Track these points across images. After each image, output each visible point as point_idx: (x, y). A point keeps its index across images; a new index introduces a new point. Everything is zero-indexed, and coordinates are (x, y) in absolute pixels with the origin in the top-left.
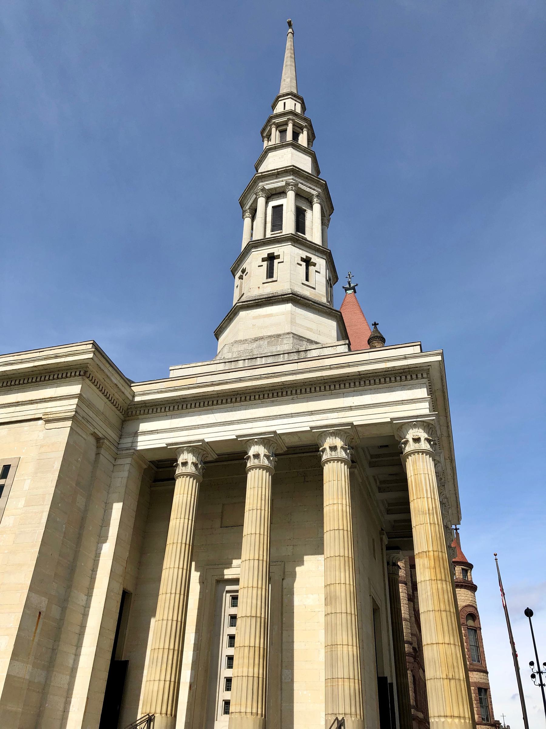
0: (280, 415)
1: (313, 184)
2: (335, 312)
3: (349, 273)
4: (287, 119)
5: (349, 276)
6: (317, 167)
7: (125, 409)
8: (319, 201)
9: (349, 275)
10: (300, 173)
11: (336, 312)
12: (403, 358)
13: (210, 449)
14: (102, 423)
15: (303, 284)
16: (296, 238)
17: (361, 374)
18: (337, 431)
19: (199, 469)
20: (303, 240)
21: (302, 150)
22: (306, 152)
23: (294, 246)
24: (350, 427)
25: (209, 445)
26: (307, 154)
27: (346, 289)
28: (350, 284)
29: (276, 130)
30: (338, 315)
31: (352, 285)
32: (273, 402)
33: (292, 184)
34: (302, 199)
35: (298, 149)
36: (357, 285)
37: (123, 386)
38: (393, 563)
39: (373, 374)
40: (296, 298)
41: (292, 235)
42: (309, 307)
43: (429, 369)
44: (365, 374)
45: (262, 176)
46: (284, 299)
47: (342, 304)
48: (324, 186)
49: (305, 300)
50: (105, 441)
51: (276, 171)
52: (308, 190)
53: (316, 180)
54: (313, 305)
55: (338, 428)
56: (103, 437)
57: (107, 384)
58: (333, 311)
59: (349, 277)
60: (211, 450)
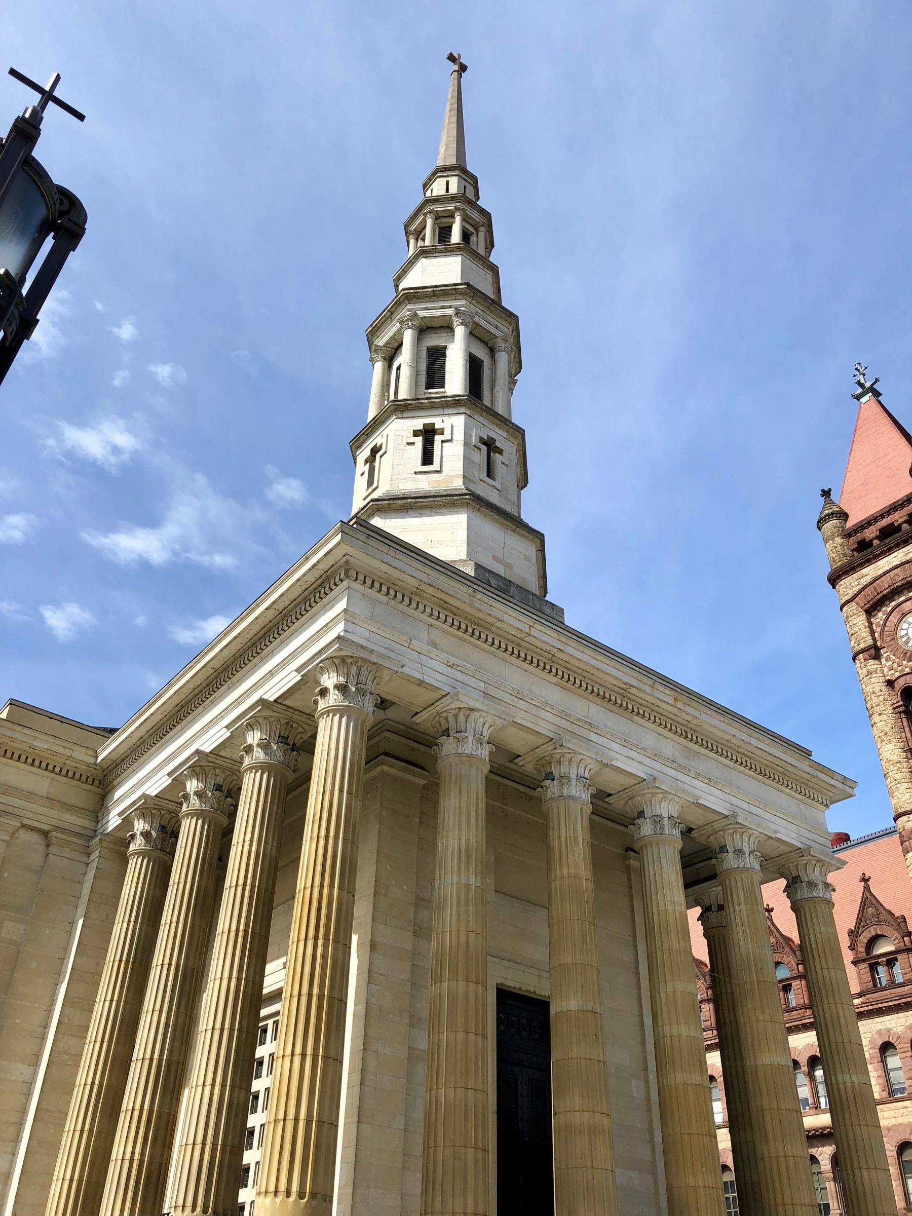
0: (211, 721)
1: (450, 299)
2: (458, 497)
3: (857, 366)
4: (453, 208)
5: (859, 371)
6: (484, 262)
8: (460, 321)
9: (856, 369)
10: (419, 294)
11: (461, 497)
13: (172, 804)
14: (46, 809)
16: (402, 405)
18: (252, 719)
20: (414, 402)
21: (442, 252)
22: (451, 251)
24: (260, 707)
25: (165, 799)
26: (452, 253)
27: (858, 397)
28: (861, 385)
29: (417, 240)
30: (468, 501)
31: (868, 385)
32: (212, 702)
33: (406, 318)
34: (439, 332)
36: (877, 380)
37: (65, 748)
39: (294, 603)
40: (381, 504)
41: (392, 403)
42: (411, 509)
43: (347, 561)
44: (285, 608)
45: (374, 330)
46: (368, 513)
47: (856, 427)
49: (397, 501)
50: (54, 834)
51: (386, 311)
52: (440, 312)
53: (449, 290)
54: (416, 503)
55: (251, 715)
58: (456, 498)
59: (858, 373)
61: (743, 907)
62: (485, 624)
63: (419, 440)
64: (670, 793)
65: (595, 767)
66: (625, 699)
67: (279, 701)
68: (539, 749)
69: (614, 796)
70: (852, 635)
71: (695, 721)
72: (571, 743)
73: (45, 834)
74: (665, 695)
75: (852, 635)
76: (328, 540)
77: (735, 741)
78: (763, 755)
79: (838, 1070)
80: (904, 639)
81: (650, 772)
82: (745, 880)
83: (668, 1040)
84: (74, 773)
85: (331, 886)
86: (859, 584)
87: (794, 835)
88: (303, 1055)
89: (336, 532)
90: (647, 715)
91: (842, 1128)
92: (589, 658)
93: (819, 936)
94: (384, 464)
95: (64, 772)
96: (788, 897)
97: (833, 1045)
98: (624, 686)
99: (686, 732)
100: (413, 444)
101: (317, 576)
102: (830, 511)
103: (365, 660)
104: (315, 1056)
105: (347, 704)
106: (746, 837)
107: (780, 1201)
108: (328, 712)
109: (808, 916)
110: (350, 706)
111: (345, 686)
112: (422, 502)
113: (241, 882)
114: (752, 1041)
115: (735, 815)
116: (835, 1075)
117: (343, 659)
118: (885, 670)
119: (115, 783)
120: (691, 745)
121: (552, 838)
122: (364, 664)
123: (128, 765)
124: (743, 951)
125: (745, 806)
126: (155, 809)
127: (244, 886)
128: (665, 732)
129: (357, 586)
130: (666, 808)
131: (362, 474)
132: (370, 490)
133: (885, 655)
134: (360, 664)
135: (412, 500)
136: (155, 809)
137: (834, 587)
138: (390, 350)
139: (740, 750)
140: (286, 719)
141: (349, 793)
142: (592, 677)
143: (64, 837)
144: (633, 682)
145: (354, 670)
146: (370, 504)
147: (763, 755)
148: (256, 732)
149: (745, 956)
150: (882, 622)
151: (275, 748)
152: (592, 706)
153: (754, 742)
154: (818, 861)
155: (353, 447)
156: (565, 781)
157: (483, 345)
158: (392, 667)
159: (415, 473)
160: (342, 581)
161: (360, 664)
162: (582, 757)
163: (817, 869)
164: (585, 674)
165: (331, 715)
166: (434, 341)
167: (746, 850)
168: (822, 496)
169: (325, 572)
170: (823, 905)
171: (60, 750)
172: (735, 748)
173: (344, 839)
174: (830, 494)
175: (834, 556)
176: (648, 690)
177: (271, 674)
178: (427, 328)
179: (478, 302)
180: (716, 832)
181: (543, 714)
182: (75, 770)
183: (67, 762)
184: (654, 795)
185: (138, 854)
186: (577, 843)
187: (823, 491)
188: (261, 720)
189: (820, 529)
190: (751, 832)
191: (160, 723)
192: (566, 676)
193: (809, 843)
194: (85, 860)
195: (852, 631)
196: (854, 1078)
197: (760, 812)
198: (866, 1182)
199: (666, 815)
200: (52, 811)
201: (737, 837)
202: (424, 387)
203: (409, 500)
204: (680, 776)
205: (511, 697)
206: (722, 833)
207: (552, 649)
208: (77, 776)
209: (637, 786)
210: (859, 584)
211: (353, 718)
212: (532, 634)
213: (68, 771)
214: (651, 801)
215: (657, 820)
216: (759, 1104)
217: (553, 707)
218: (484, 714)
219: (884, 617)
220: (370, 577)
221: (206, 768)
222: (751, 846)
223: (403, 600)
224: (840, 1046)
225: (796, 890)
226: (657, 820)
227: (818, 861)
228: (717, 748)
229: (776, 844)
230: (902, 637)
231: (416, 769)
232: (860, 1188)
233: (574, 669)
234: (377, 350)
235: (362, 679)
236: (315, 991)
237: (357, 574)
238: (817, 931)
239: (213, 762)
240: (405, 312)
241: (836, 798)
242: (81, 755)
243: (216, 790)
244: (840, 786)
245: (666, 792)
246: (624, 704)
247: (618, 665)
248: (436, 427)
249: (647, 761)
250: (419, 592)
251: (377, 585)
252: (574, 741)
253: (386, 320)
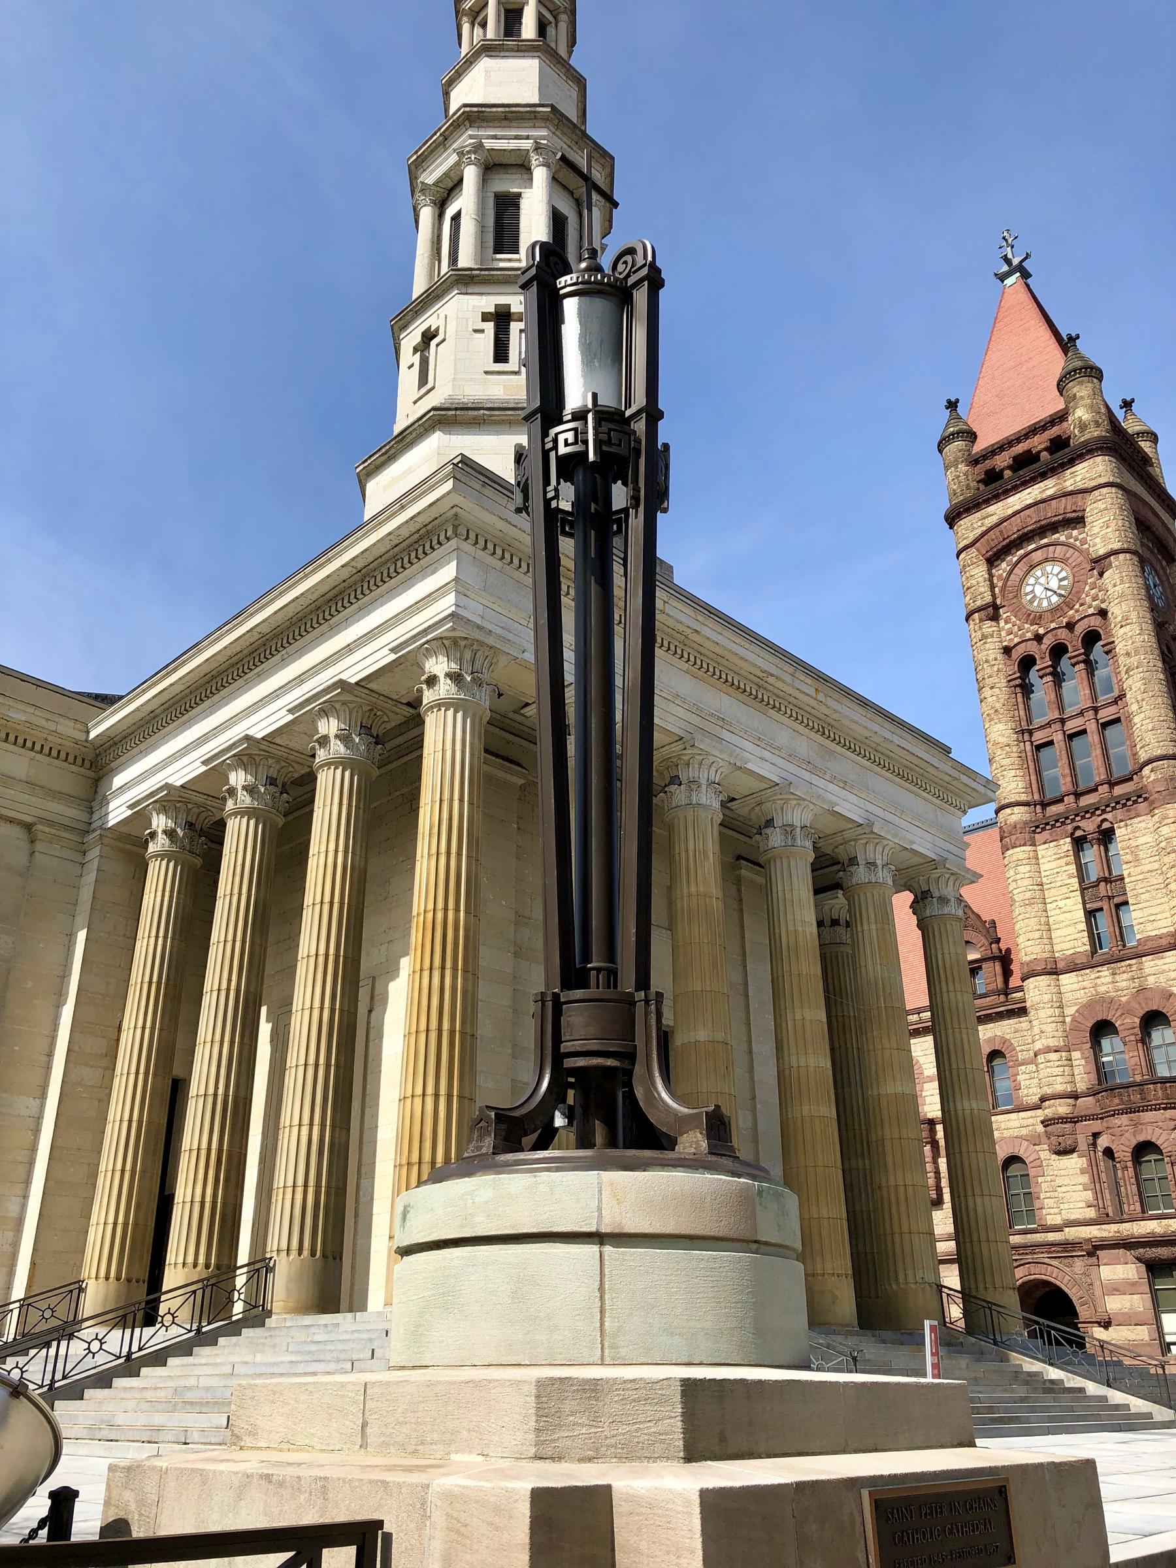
0: (261, 700)
5: (1006, 241)
6: (568, 70)
7: (91, 756)
9: (1004, 238)
12: (400, 509)
14: (27, 796)
15: (486, 373)
16: (467, 275)
17: (359, 569)
19: (182, 840)
20: (483, 273)
21: (512, 50)
23: (467, 294)
26: (526, 54)
27: (1002, 278)
28: (1007, 260)
29: (473, 25)
31: (1016, 261)
32: (258, 675)
33: (467, 149)
34: (510, 171)
35: (502, 54)
36: (1028, 256)
38: (832, 920)
39: (376, 562)
42: (484, 423)
43: (456, 515)
45: (419, 159)
46: (426, 425)
47: (996, 318)
48: (552, 116)
49: (466, 412)
50: (40, 827)
51: (438, 134)
52: (513, 144)
53: (526, 112)
54: (491, 416)
55: (325, 698)
56: (35, 820)
57: (13, 725)
59: (1005, 244)
60: (205, 797)
61: (873, 927)
63: (490, 327)
64: (805, 800)
65: (725, 770)
66: (761, 690)
67: (362, 684)
68: (664, 749)
69: (739, 801)
70: (968, 589)
71: (835, 716)
72: (703, 744)
73: (28, 827)
74: (807, 685)
75: (968, 589)
76: (434, 486)
77: (875, 739)
78: (903, 753)
79: (958, 1097)
80: (1029, 597)
81: (784, 775)
82: (876, 896)
83: (794, 1071)
84: (59, 752)
85: (457, 910)
86: (983, 525)
87: (929, 846)
88: (437, 1095)
89: (445, 477)
90: (783, 708)
91: (958, 1155)
92: (727, 641)
93: (947, 956)
94: (442, 356)
95: (46, 750)
96: (914, 913)
97: (954, 1072)
98: (761, 675)
99: (823, 728)
100: (482, 331)
101: (414, 530)
102: (956, 429)
103: (481, 643)
104: (449, 1096)
105: (462, 697)
106: (879, 848)
107: (896, 1230)
108: (439, 705)
109: (937, 933)
110: (466, 700)
111: (460, 675)
112: (499, 415)
113: (327, 899)
114: (876, 1071)
115: (871, 824)
116: (954, 1102)
117: (455, 641)
118: (1003, 633)
119: (113, 765)
120: (827, 743)
121: (677, 852)
122: (479, 647)
123: (133, 745)
124: (871, 975)
125: (879, 812)
126: (180, 802)
127: (332, 903)
128: (801, 728)
129: (467, 547)
130: (798, 817)
131: (410, 367)
132: (423, 390)
133: (1005, 616)
134: (475, 647)
135: (486, 412)
136: (180, 802)
137: (951, 527)
138: (442, 190)
139: (879, 748)
140: (368, 705)
141: (471, 803)
142: (726, 663)
143: (53, 831)
144: (773, 670)
145: (468, 655)
146: (431, 414)
147: (903, 753)
148: (331, 719)
149: (872, 981)
150: (1004, 574)
151: (357, 740)
152: (725, 698)
153: (897, 740)
154: (952, 874)
155: (396, 328)
156: (694, 787)
157: (567, 195)
158: (511, 652)
159: (486, 373)
160: (448, 539)
161: (475, 647)
162: (713, 759)
163: (951, 883)
164: (719, 659)
165: (443, 709)
166: (507, 184)
167: (879, 862)
168: (947, 408)
169: (425, 526)
170: (954, 923)
171: (43, 723)
172: (874, 746)
173: (468, 857)
174: (957, 407)
175: (955, 487)
176: (788, 679)
177: (349, 649)
178: (495, 165)
179: (564, 134)
180: (846, 842)
182: (60, 748)
183: (50, 738)
184: (786, 801)
185: (161, 856)
186: (706, 857)
187: (949, 402)
188: (338, 706)
189: (940, 451)
190: (886, 842)
191: (180, 695)
192: (699, 662)
193: (945, 855)
194: (79, 858)
195: (969, 584)
196: (974, 1105)
197: (896, 820)
198: (980, 1209)
199: (799, 825)
200: (34, 799)
201: (870, 847)
202: (491, 250)
203: (482, 412)
204: (815, 780)
206: (853, 843)
207: (685, 629)
208: (62, 755)
209: (770, 790)
210: (983, 525)
211: (470, 714)
212: (666, 611)
213: (51, 749)
214: (782, 809)
215: (789, 829)
216: (880, 1133)
217: (684, 700)
219: (1008, 568)
220: (483, 536)
221: (256, 758)
222: (885, 858)
223: (520, 567)
224: (962, 1073)
225: (925, 906)
226: (789, 829)
227: (952, 874)
228: (855, 747)
229: (910, 855)
230: (1027, 594)
231: (513, 766)
232: (972, 1214)
233: (708, 653)
234: (425, 188)
235: (477, 666)
236: (446, 1026)
237: (468, 531)
238: (946, 951)
239: (265, 751)
240: (465, 139)
241: (973, 803)
242: (68, 729)
243: (271, 784)
244: (982, 789)
245: (800, 798)
246: (760, 696)
247: (758, 650)
248: (512, 311)
249: (781, 762)
251: (490, 546)
252: (707, 741)
253: (436, 147)
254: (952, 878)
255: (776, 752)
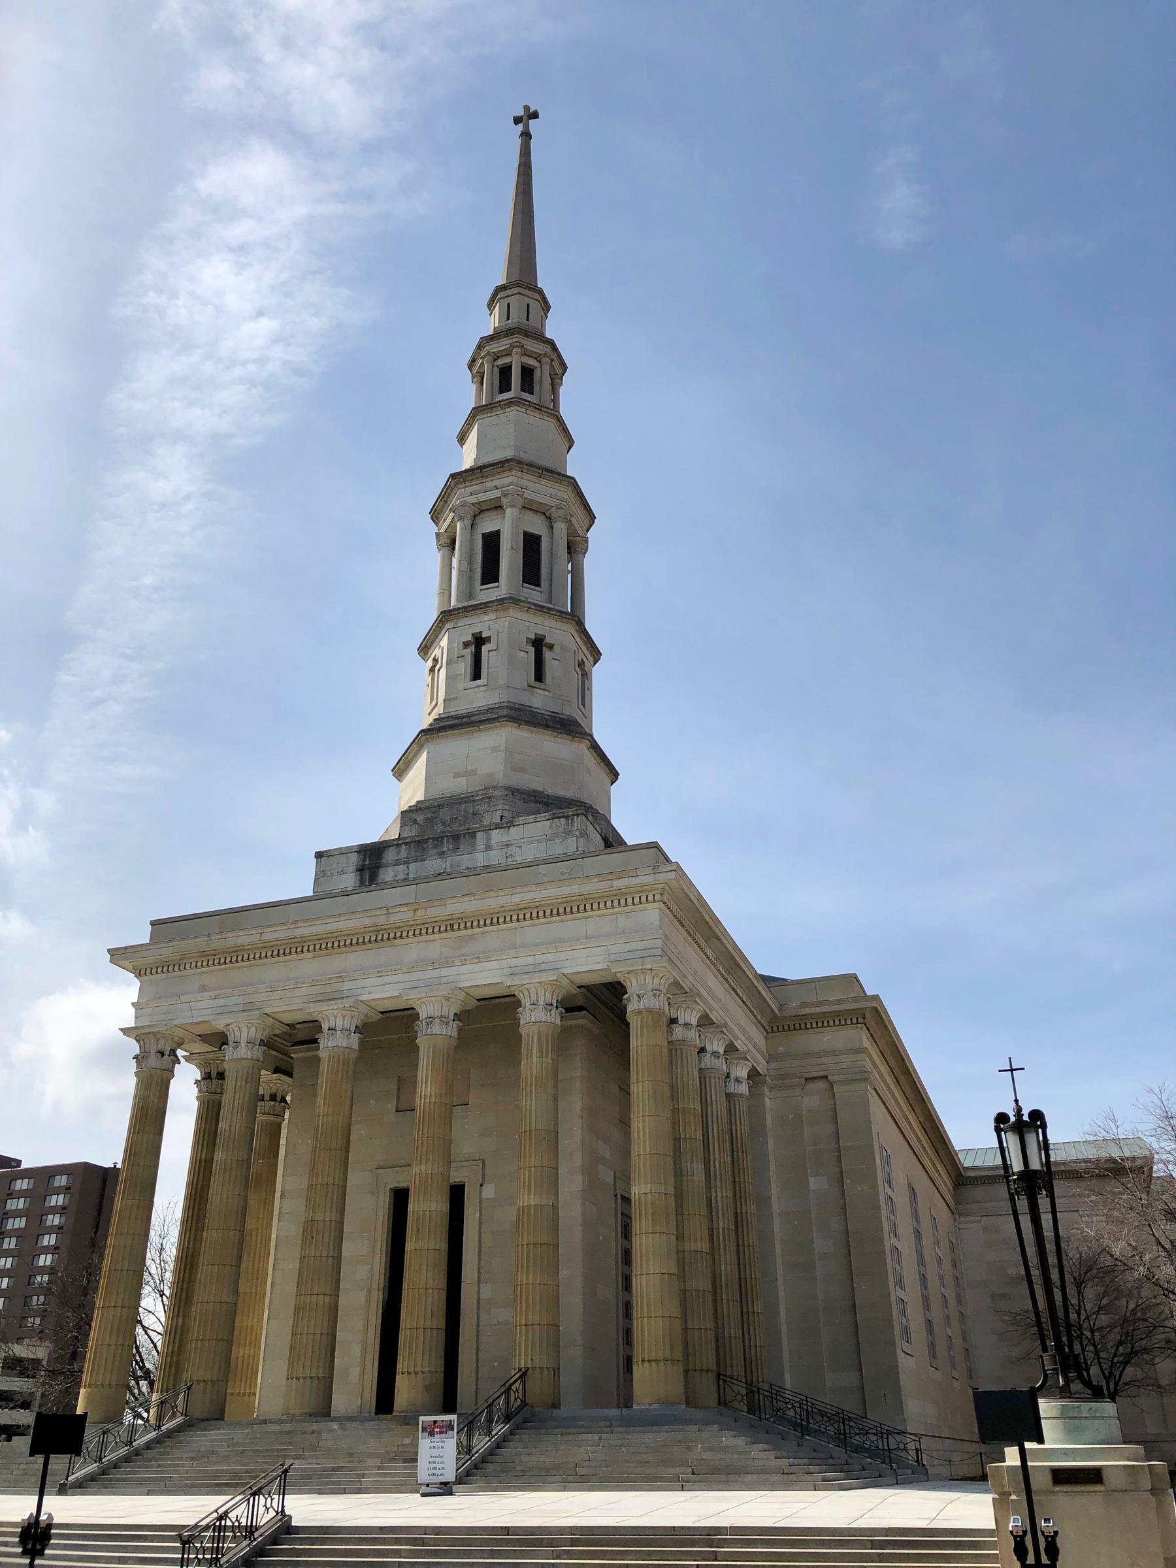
21: (469, 428)
38: (671, 1019)
62: (238, 948)
106: (526, 993)
135: (403, 758)
139: (520, 907)
142: (342, 933)
162: (326, 1013)
181: (297, 992)
204: (445, 972)
205: (267, 994)
218: (235, 1024)
250: (183, 957)
254: (631, 975)
255: (400, 972)
